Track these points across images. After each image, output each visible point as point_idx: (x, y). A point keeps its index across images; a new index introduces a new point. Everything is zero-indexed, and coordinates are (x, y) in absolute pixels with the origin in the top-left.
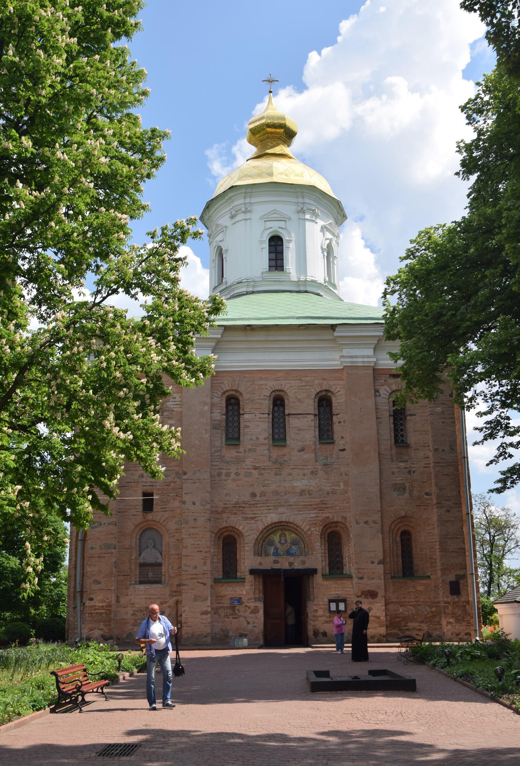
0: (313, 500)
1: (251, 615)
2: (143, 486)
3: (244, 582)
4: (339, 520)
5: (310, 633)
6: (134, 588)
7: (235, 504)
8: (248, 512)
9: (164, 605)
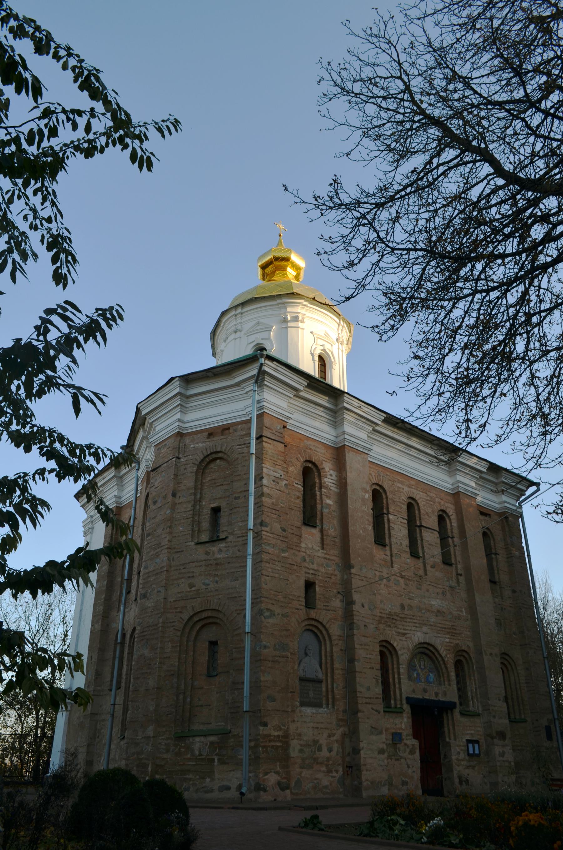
0: (447, 623)
1: (410, 756)
2: (306, 573)
3: (402, 712)
4: (466, 649)
6: (300, 711)
7: (389, 615)
8: (400, 627)
9: (332, 739)
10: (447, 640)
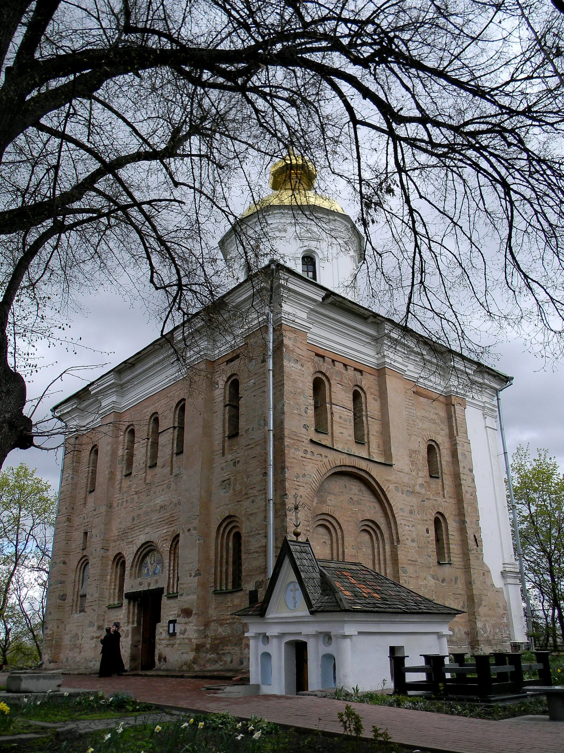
5: (156, 658)
10: (165, 531)
